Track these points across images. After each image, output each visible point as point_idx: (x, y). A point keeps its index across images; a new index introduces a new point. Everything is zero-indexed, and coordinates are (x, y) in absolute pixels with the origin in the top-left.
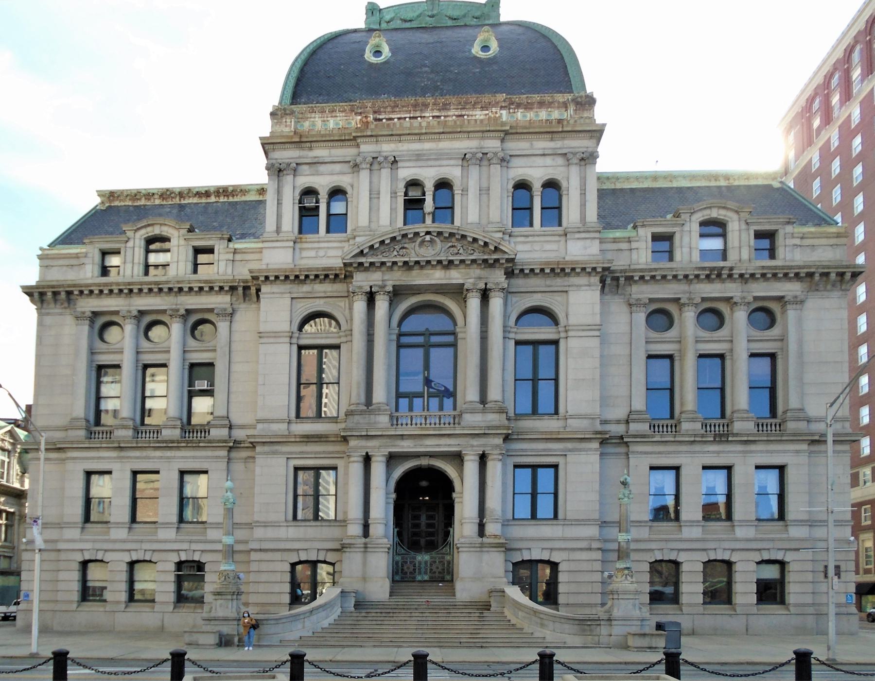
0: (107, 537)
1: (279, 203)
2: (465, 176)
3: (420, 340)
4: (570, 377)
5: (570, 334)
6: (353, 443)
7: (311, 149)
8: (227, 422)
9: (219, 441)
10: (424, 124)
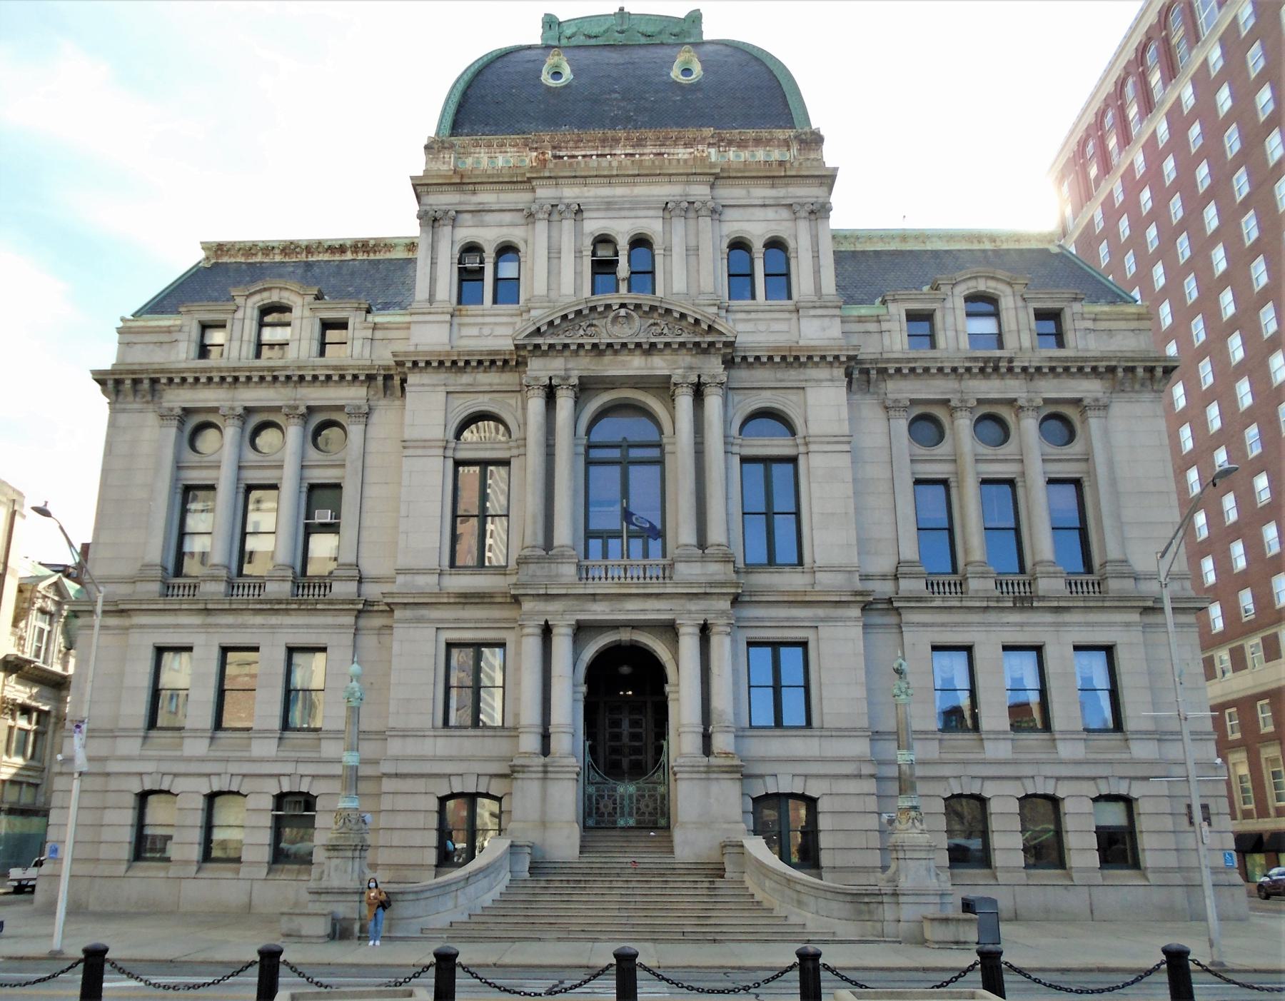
0: (178, 753)
1: (433, 263)
2: (667, 231)
3: (615, 454)
4: (815, 510)
5: (812, 447)
6: (527, 605)
7: (474, 192)
8: (355, 573)
9: (344, 602)
10: (615, 164)
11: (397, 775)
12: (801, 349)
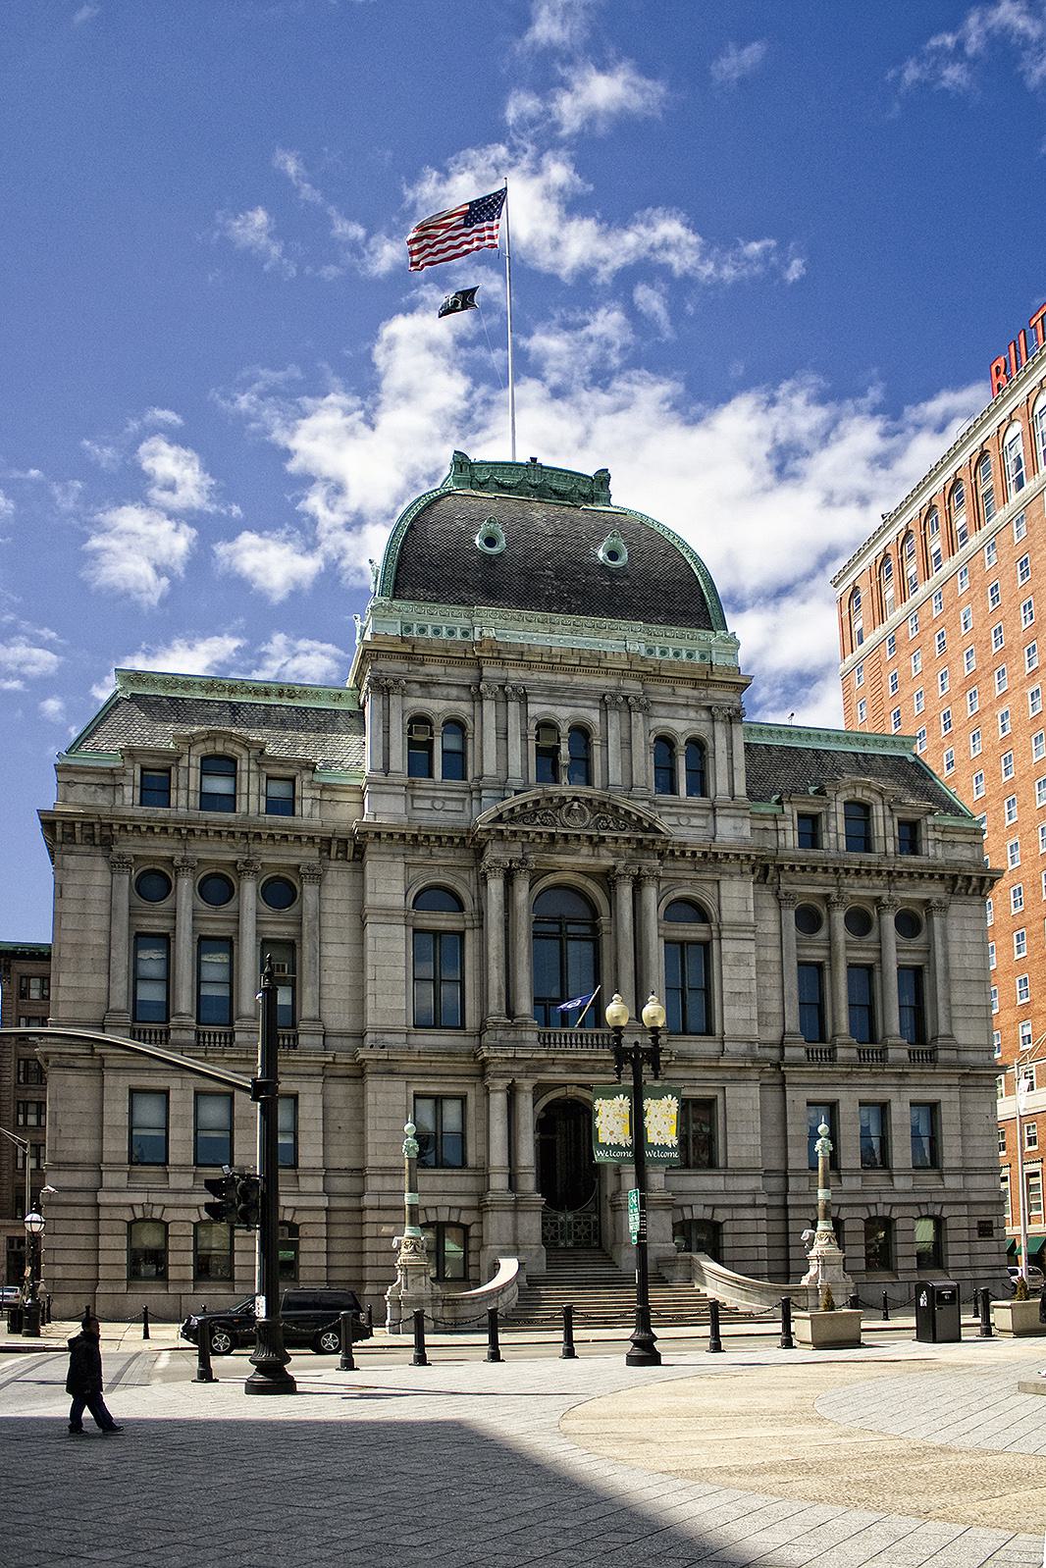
3: (555, 928)
4: (726, 988)
11: (378, 1208)
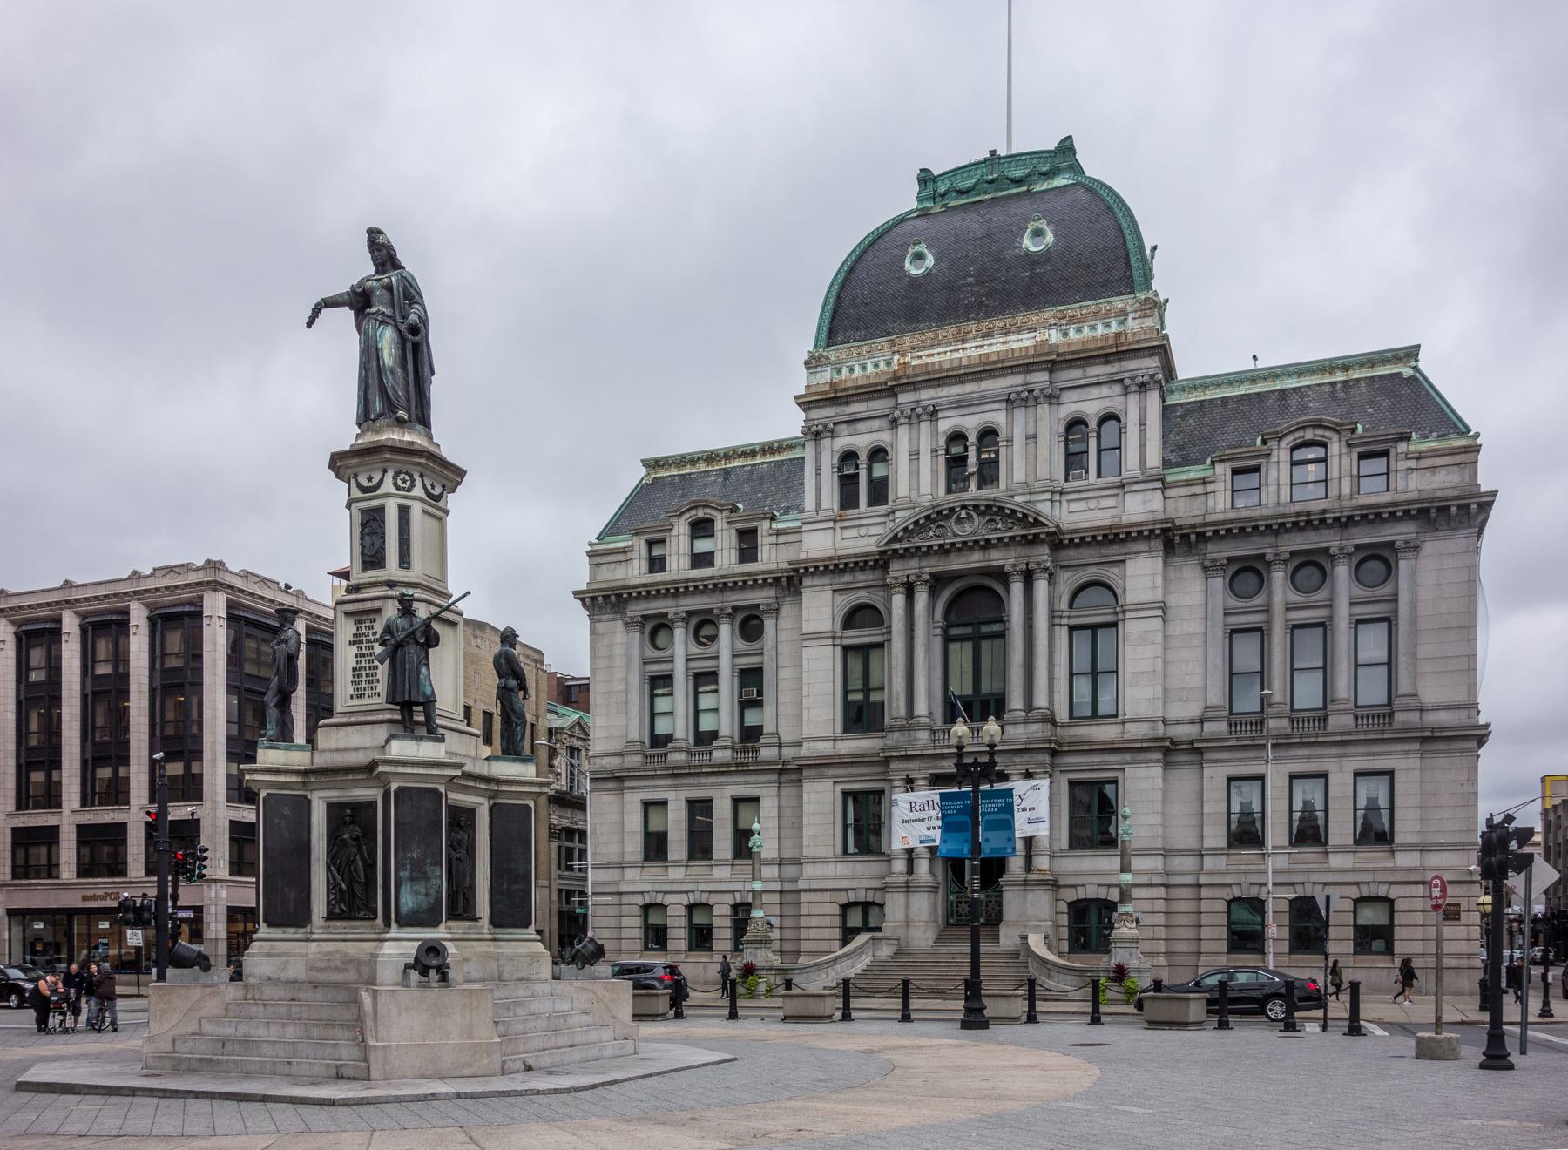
1: (818, 474)
2: (1010, 423)
6: (894, 765)
7: (847, 403)
11: (810, 890)
12: (1120, 526)
